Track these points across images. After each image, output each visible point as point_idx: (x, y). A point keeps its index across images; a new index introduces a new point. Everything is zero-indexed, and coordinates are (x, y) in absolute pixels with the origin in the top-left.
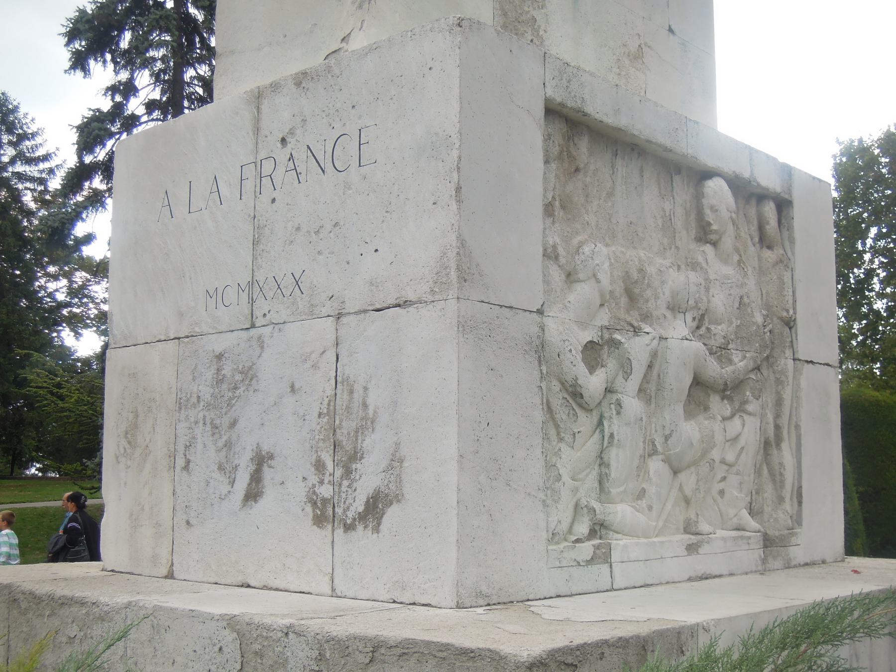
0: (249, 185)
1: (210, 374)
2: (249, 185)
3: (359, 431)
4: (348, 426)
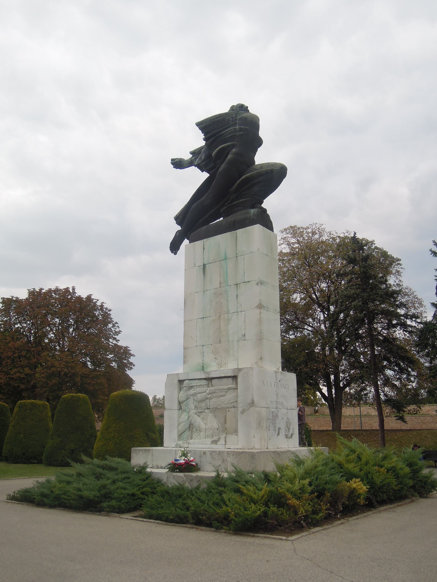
0: (276, 386)
1: (271, 415)
2: (276, 386)
3: (290, 425)
4: (289, 424)
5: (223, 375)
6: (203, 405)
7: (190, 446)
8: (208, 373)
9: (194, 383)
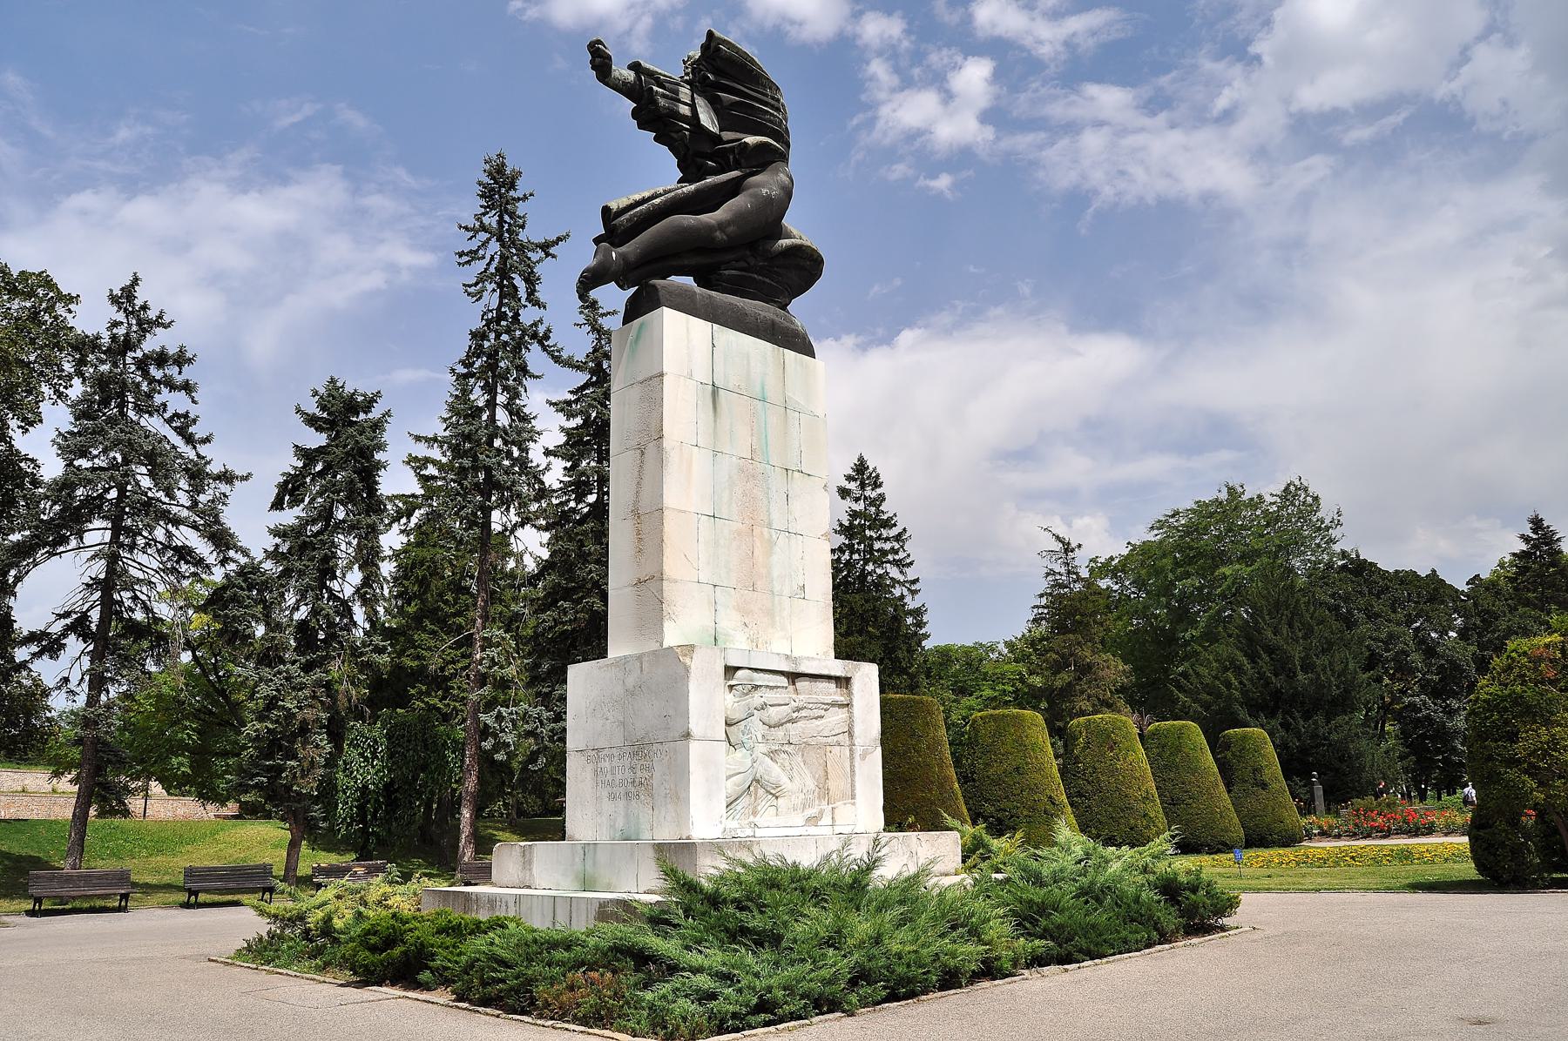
5: (825, 672)
6: (779, 733)
7: (759, 833)
8: (795, 661)
9: (761, 679)
